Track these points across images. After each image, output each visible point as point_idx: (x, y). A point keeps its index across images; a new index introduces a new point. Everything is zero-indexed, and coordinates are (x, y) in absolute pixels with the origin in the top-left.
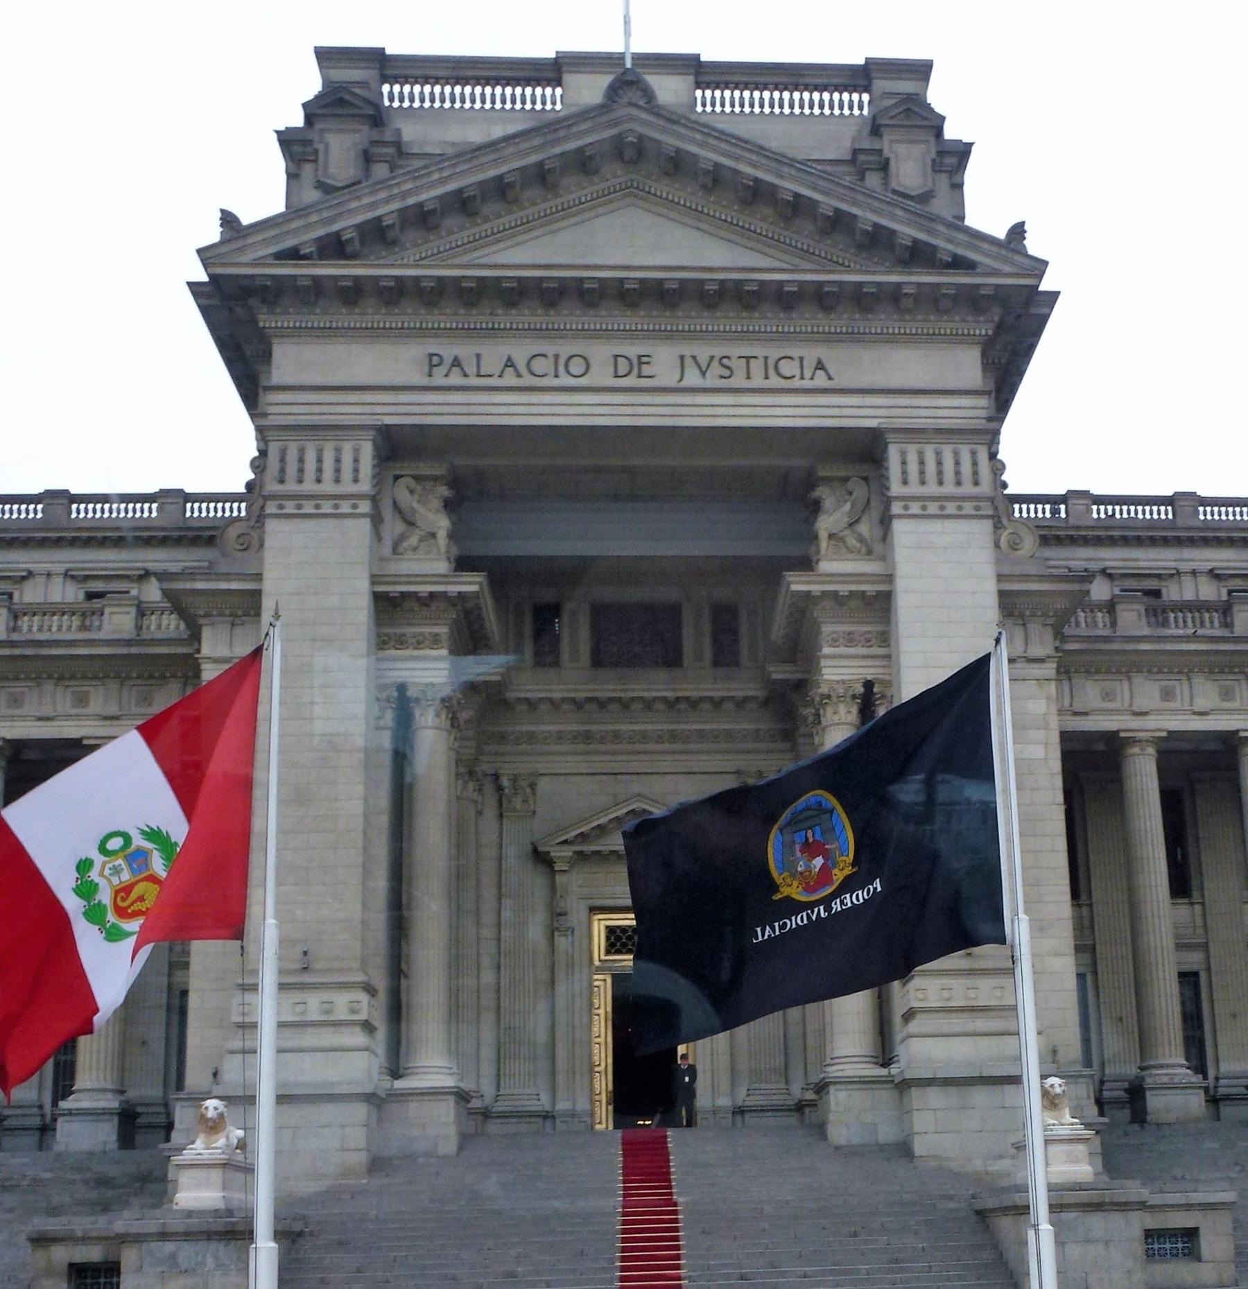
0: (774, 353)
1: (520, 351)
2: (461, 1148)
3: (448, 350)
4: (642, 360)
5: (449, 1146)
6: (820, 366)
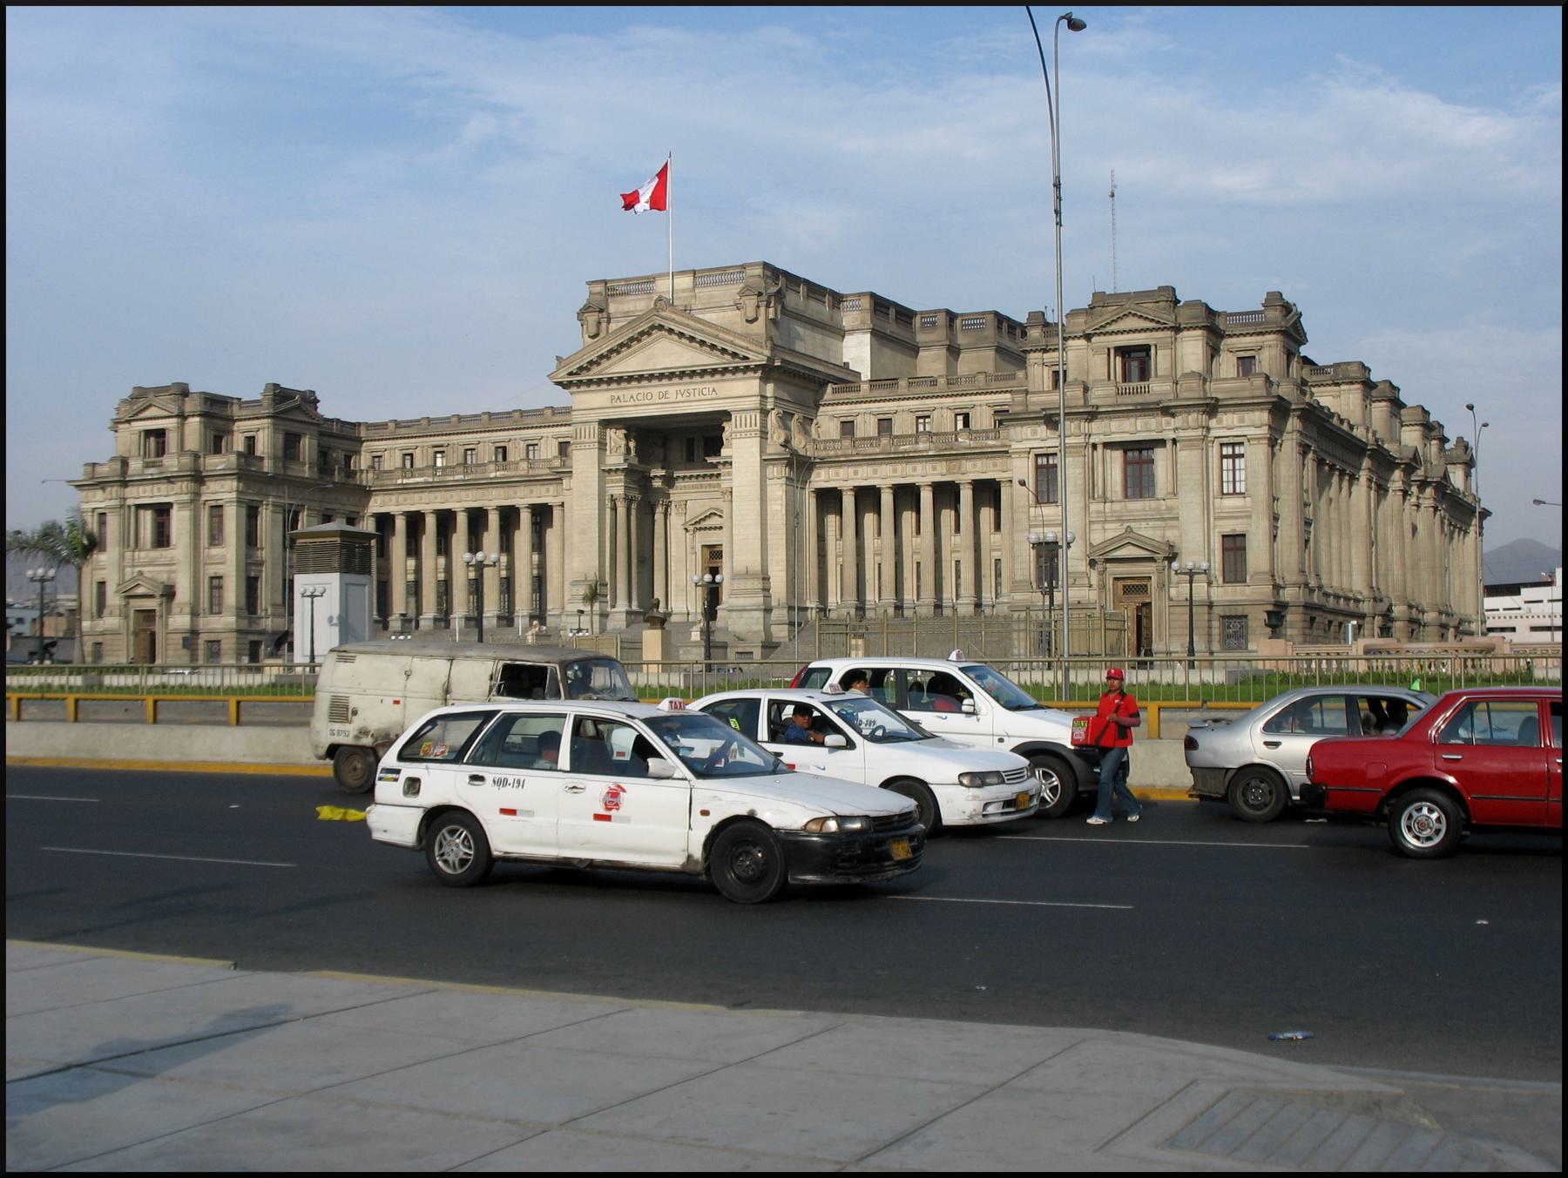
0: (701, 387)
1: (634, 392)
2: (628, 626)
5: (624, 627)
6: (714, 390)
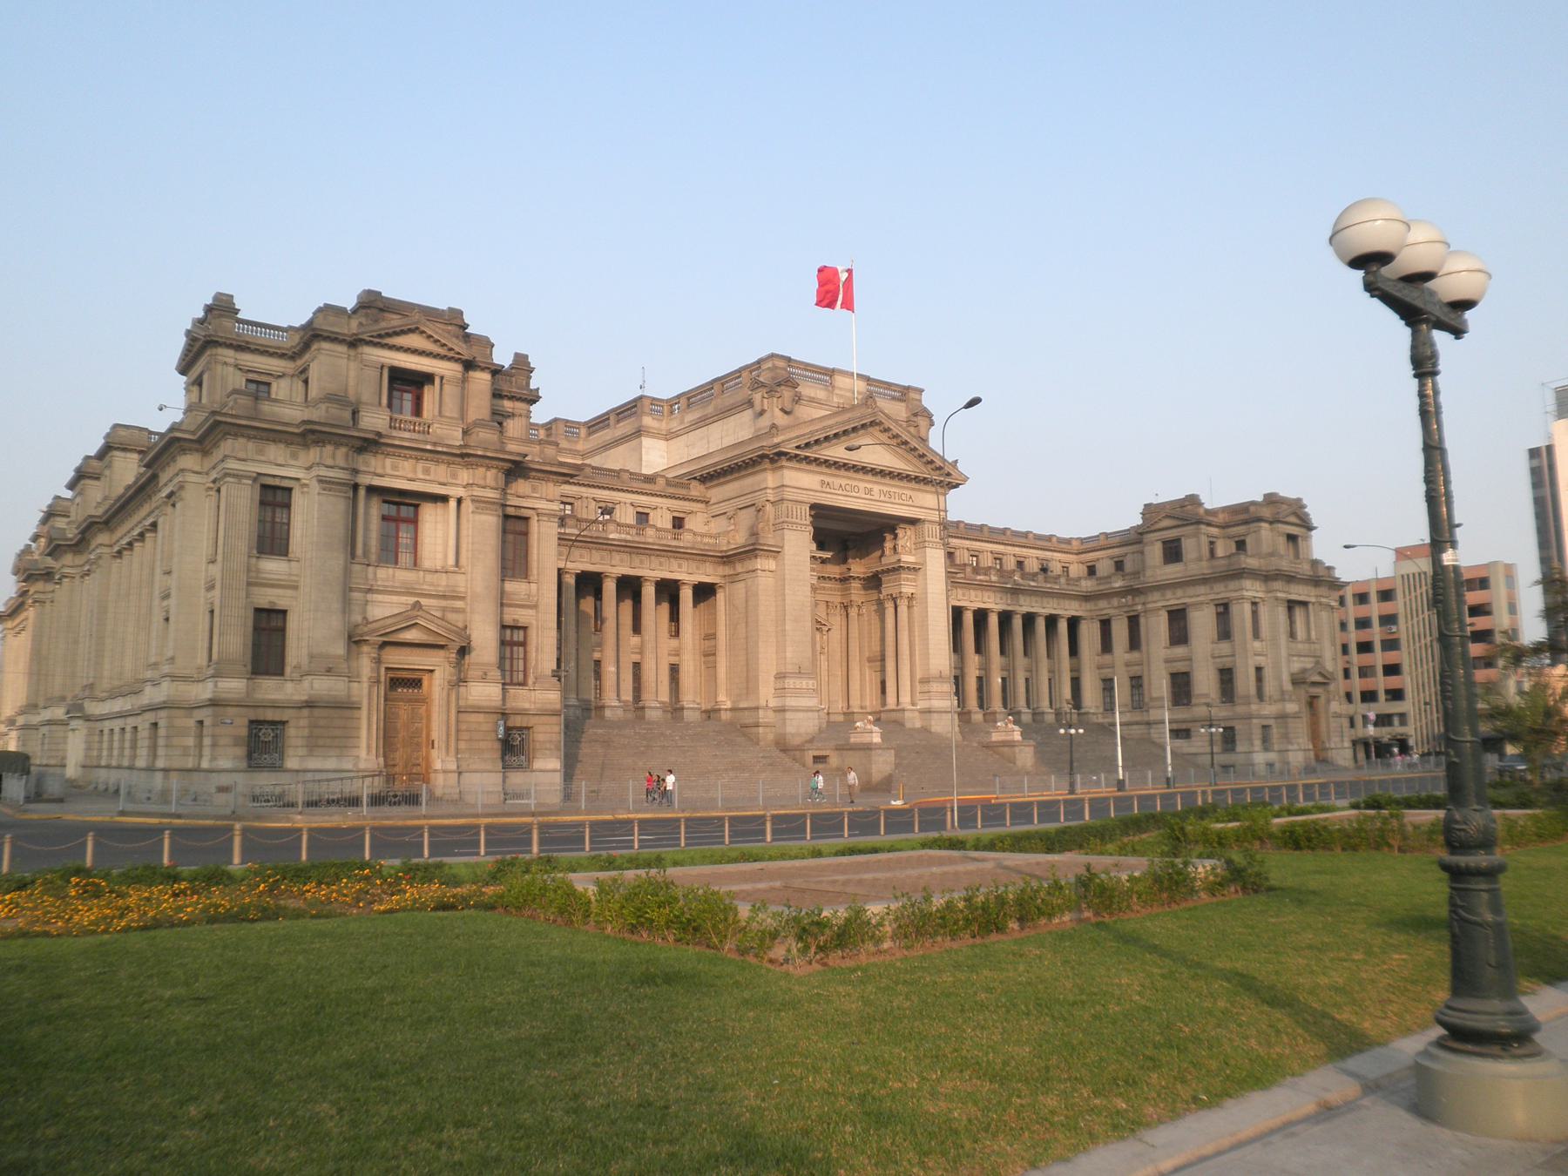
1: (844, 482)
3: (827, 479)
4: (871, 490)
